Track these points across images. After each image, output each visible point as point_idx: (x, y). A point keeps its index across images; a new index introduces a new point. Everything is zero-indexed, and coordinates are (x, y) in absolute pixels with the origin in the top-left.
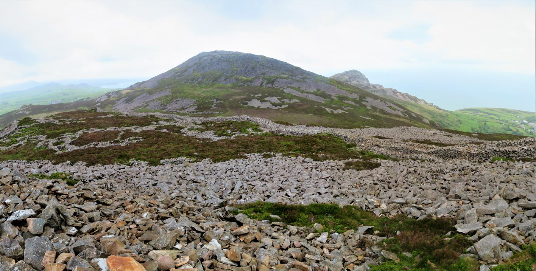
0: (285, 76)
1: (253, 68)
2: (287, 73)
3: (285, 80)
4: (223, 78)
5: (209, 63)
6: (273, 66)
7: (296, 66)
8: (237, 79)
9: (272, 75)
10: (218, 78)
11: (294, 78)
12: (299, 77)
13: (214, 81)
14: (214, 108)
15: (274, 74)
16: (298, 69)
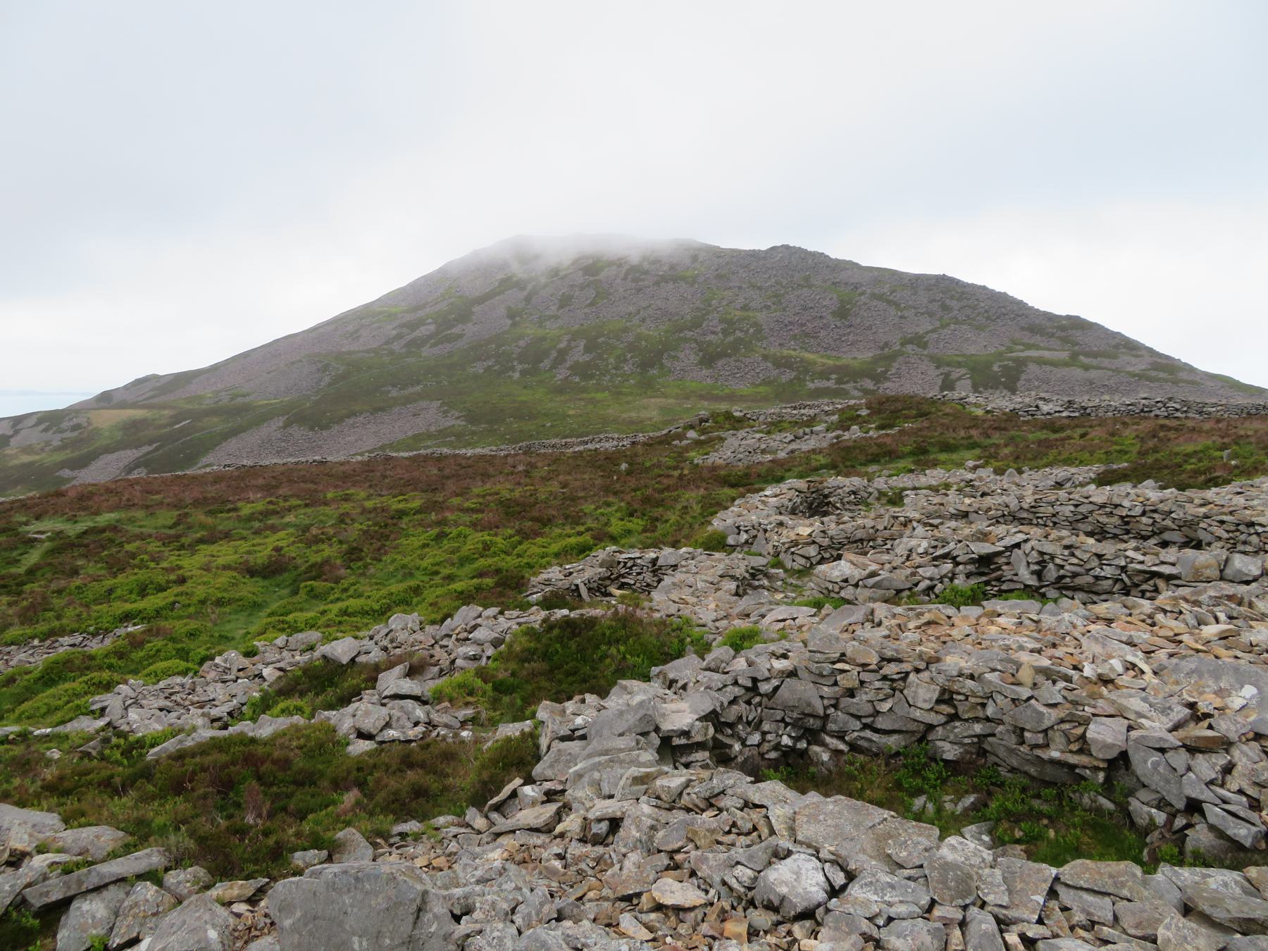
0: (1047, 354)
1: (842, 313)
2: (1037, 339)
3: (1078, 373)
4: (688, 356)
5: (582, 288)
6: (945, 308)
7: (1061, 310)
8: (783, 363)
9: (972, 350)
10: (660, 354)
11: (1106, 362)
12: (1139, 366)
13: (645, 365)
15: (978, 346)
16: (1076, 324)
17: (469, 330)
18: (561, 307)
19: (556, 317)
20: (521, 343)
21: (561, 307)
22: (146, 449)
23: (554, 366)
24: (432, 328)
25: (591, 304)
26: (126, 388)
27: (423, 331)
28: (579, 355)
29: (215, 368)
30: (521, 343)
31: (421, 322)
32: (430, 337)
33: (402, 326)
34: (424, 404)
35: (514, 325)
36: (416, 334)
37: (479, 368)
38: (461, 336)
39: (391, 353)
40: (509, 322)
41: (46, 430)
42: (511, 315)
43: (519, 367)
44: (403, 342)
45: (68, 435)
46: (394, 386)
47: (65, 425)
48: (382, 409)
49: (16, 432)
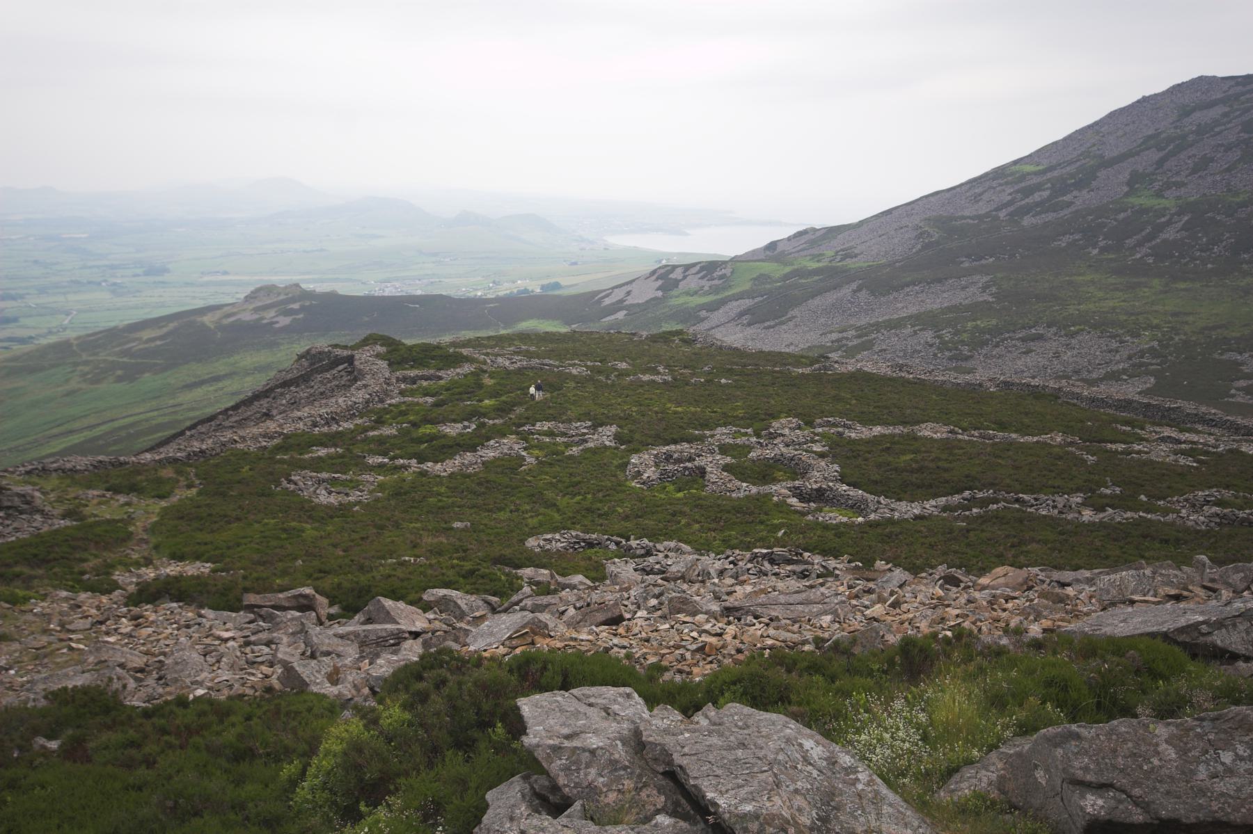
5: (1228, 148)
14: (1241, 398)
17: (1082, 199)
18: (1194, 172)
19: (1184, 184)
20: (1122, 215)
21: (1194, 172)
22: (757, 300)
23: (1140, 244)
24: (1047, 193)
25: (1228, 170)
26: (789, 239)
27: (1037, 197)
28: (1170, 234)
29: (861, 223)
30: (1122, 215)
31: (1039, 187)
32: (1037, 204)
33: (1017, 191)
34: (976, 278)
35: (1127, 195)
36: (1029, 200)
37: (1063, 242)
38: (1070, 204)
39: (997, 218)
40: (1126, 189)
41: (702, 278)
42: (1129, 183)
43: (1101, 244)
44: (1011, 209)
45: (716, 282)
46: (968, 256)
47: (718, 273)
48: (939, 281)
49: (685, 277)
